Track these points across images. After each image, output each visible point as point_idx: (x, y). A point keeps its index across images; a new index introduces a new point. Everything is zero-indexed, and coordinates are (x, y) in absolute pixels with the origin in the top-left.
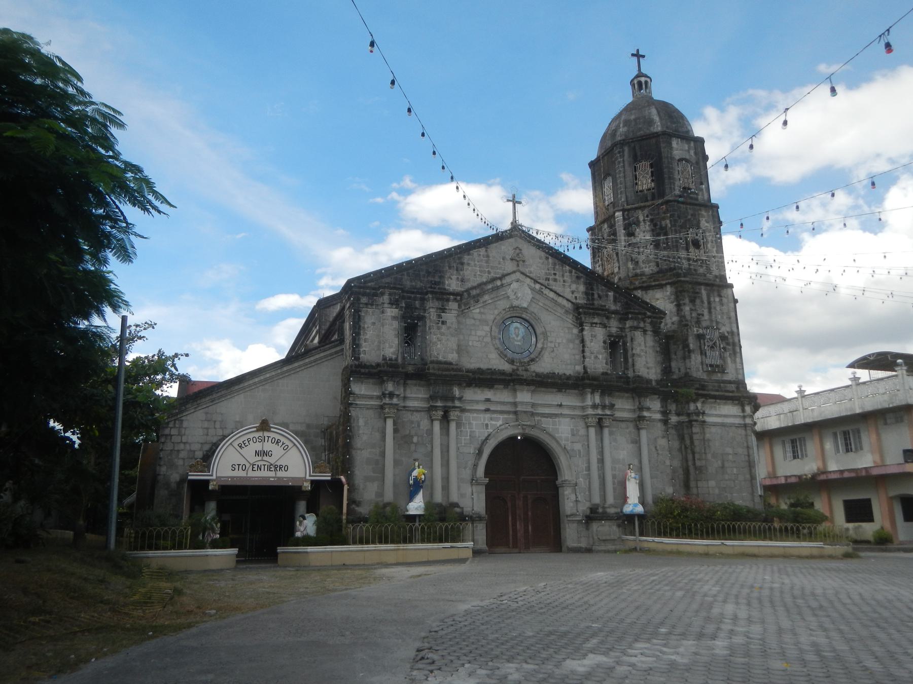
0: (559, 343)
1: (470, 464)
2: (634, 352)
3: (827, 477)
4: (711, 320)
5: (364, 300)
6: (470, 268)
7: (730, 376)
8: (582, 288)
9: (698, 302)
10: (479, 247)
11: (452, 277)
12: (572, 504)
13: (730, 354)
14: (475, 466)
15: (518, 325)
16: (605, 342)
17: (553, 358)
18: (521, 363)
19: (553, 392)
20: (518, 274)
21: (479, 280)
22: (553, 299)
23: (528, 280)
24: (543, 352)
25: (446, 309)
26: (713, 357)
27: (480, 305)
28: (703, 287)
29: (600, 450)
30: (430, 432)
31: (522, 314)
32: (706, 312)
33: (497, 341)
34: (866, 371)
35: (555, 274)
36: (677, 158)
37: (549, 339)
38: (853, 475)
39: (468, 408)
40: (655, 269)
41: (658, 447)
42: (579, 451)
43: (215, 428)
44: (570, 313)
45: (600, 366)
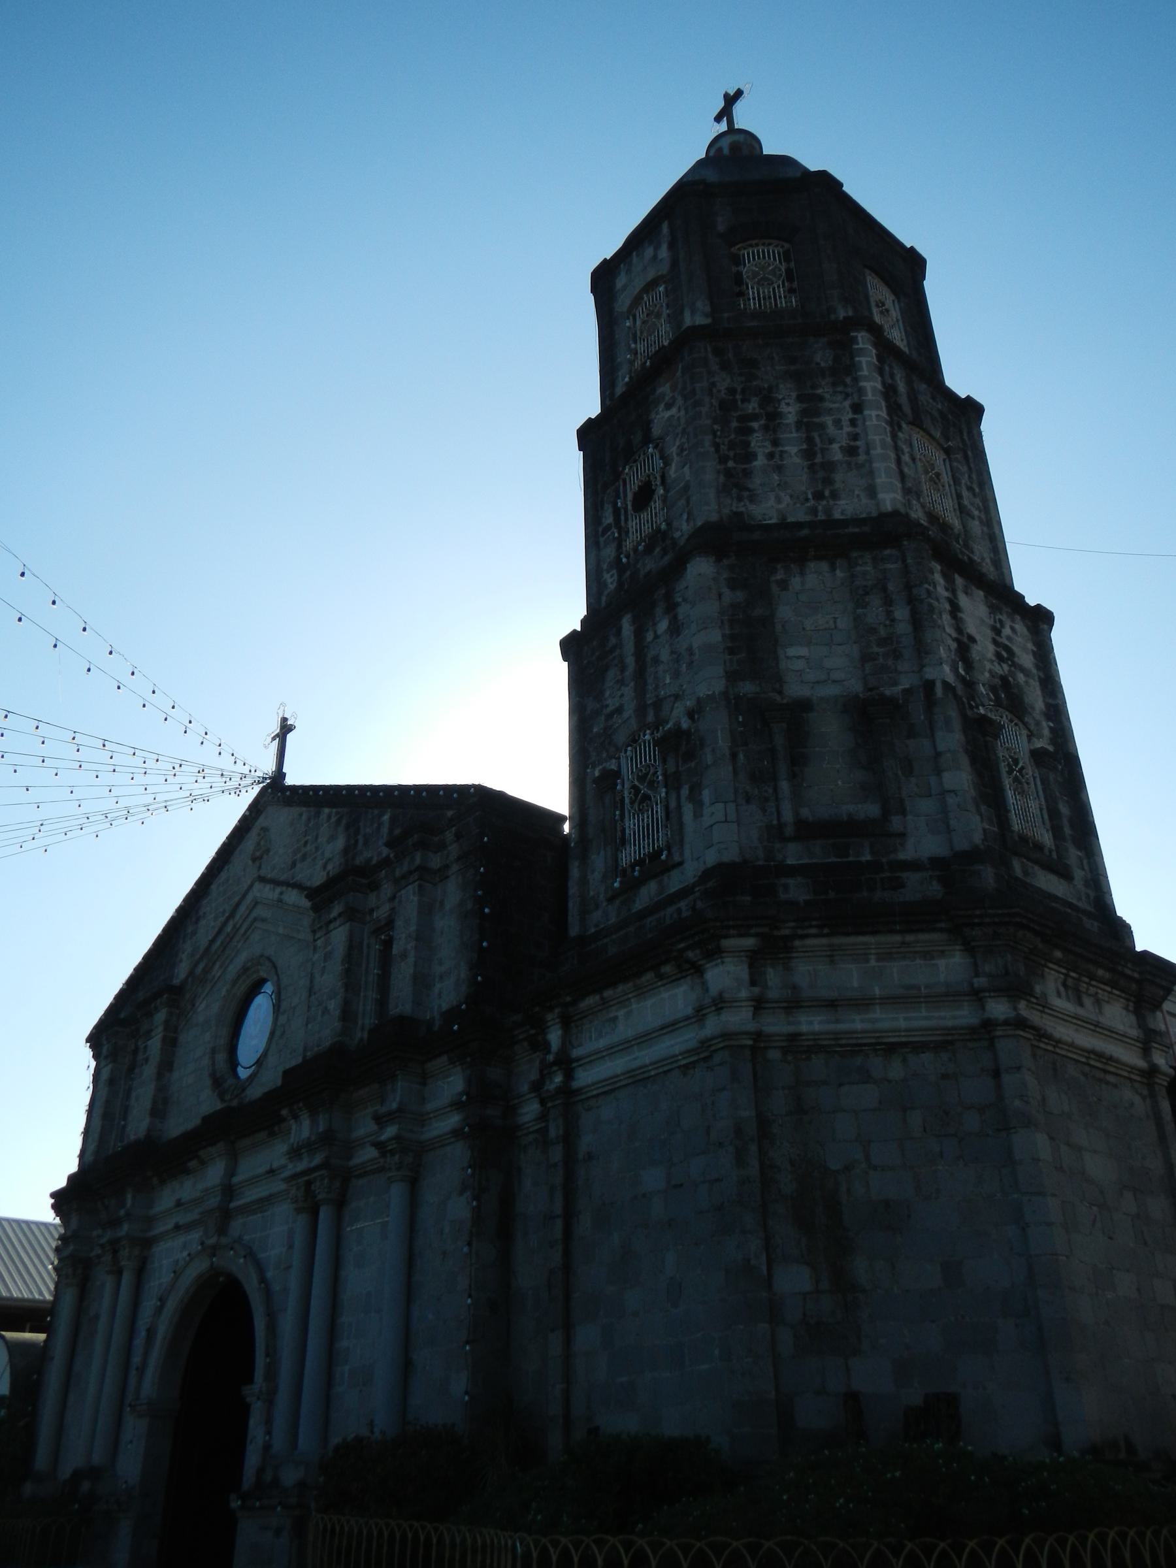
4: (641, 710)
8: (340, 843)
9: (612, 674)
13: (692, 789)
23: (268, 887)
32: (628, 691)
33: (221, 1057)
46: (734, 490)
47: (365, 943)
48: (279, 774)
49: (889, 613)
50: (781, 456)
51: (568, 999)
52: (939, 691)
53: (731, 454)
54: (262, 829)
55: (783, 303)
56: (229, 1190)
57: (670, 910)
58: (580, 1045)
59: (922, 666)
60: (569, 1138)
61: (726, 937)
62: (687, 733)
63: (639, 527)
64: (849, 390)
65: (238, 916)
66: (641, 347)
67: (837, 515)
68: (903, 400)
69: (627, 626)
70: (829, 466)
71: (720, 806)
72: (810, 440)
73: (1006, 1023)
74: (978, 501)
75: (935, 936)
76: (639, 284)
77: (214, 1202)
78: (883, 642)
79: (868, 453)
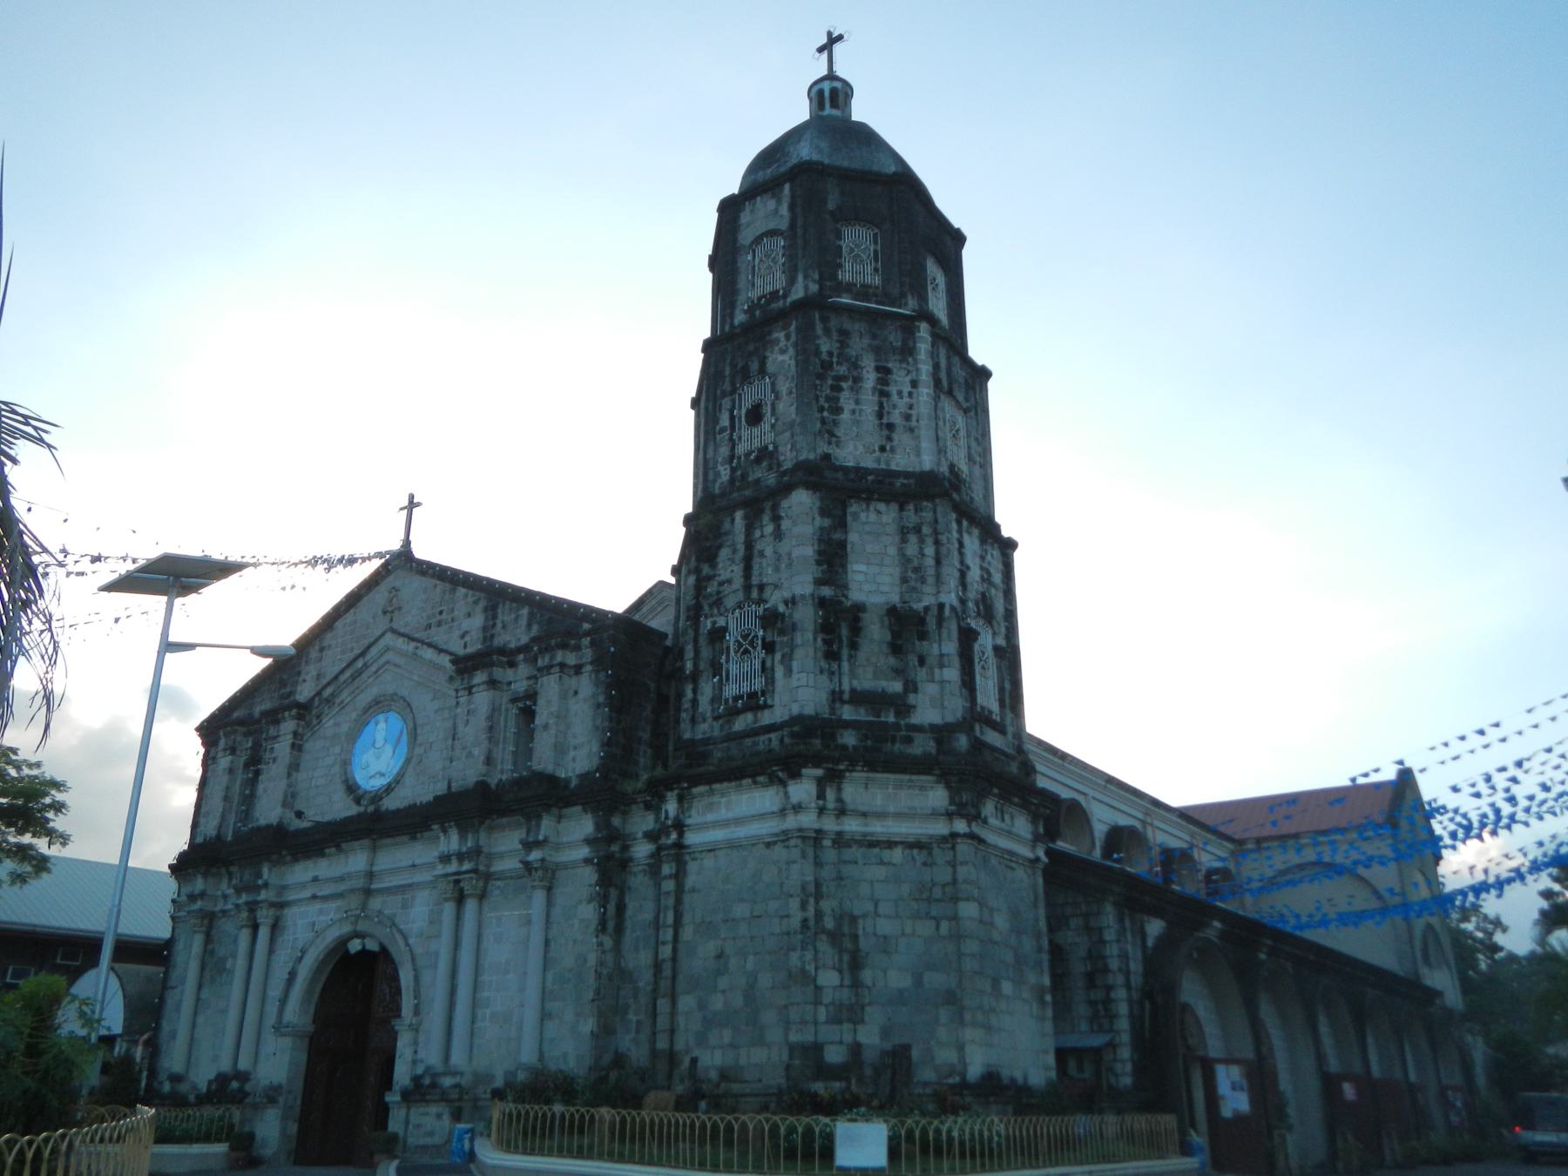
0: (432, 743)
4: (747, 588)
6: (330, 653)
8: (478, 621)
9: (724, 553)
10: (347, 611)
13: (783, 656)
14: (283, 1001)
16: (490, 717)
20: (389, 638)
21: (337, 669)
22: (431, 662)
23: (401, 639)
27: (334, 712)
28: (739, 515)
32: (737, 570)
36: (747, 242)
37: (418, 742)
39: (291, 898)
46: (826, 435)
47: (503, 707)
48: (407, 543)
49: (921, 549)
50: (860, 414)
51: (686, 785)
52: (947, 612)
53: (826, 405)
55: (869, 280)
56: (370, 875)
57: (763, 738)
58: (690, 817)
59: (939, 592)
60: (679, 876)
61: (805, 767)
62: (783, 615)
63: (750, 440)
64: (910, 368)
65: (368, 657)
66: (758, 282)
67: (893, 467)
68: (943, 375)
69: (739, 515)
70: (890, 427)
71: (805, 674)
72: (881, 406)
73: (965, 835)
74: (980, 449)
75: (930, 778)
76: (760, 227)
77: (360, 883)
78: (917, 570)
79: (918, 421)
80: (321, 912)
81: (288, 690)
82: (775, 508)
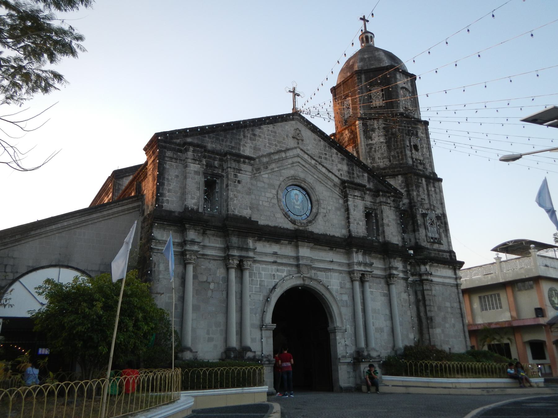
0: (329, 210)
1: (259, 310)
2: (384, 221)
3: (478, 328)
4: (430, 205)
5: (169, 154)
6: (261, 140)
7: (444, 247)
9: (421, 189)
10: (268, 124)
11: (246, 144)
12: (342, 348)
13: (443, 230)
14: (264, 312)
15: (297, 192)
17: (325, 222)
18: (301, 223)
19: (325, 250)
20: (298, 150)
21: (268, 151)
23: (306, 156)
24: (318, 215)
25: (241, 170)
26: (433, 232)
28: (424, 180)
29: (362, 301)
30: (227, 280)
31: (301, 183)
34: (504, 254)
35: (326, 154)
36: (401, 86)
37: (322, 206)
38: (498, 326)
40: (388, 163)
41: (402, 300)
42: (346, 301)
43: (5, 272)
44: (338, 186)
45: (361, 231)
54: (298, 129)
80: (278, 270)
81: (233, 145)
82: (433, 183)
